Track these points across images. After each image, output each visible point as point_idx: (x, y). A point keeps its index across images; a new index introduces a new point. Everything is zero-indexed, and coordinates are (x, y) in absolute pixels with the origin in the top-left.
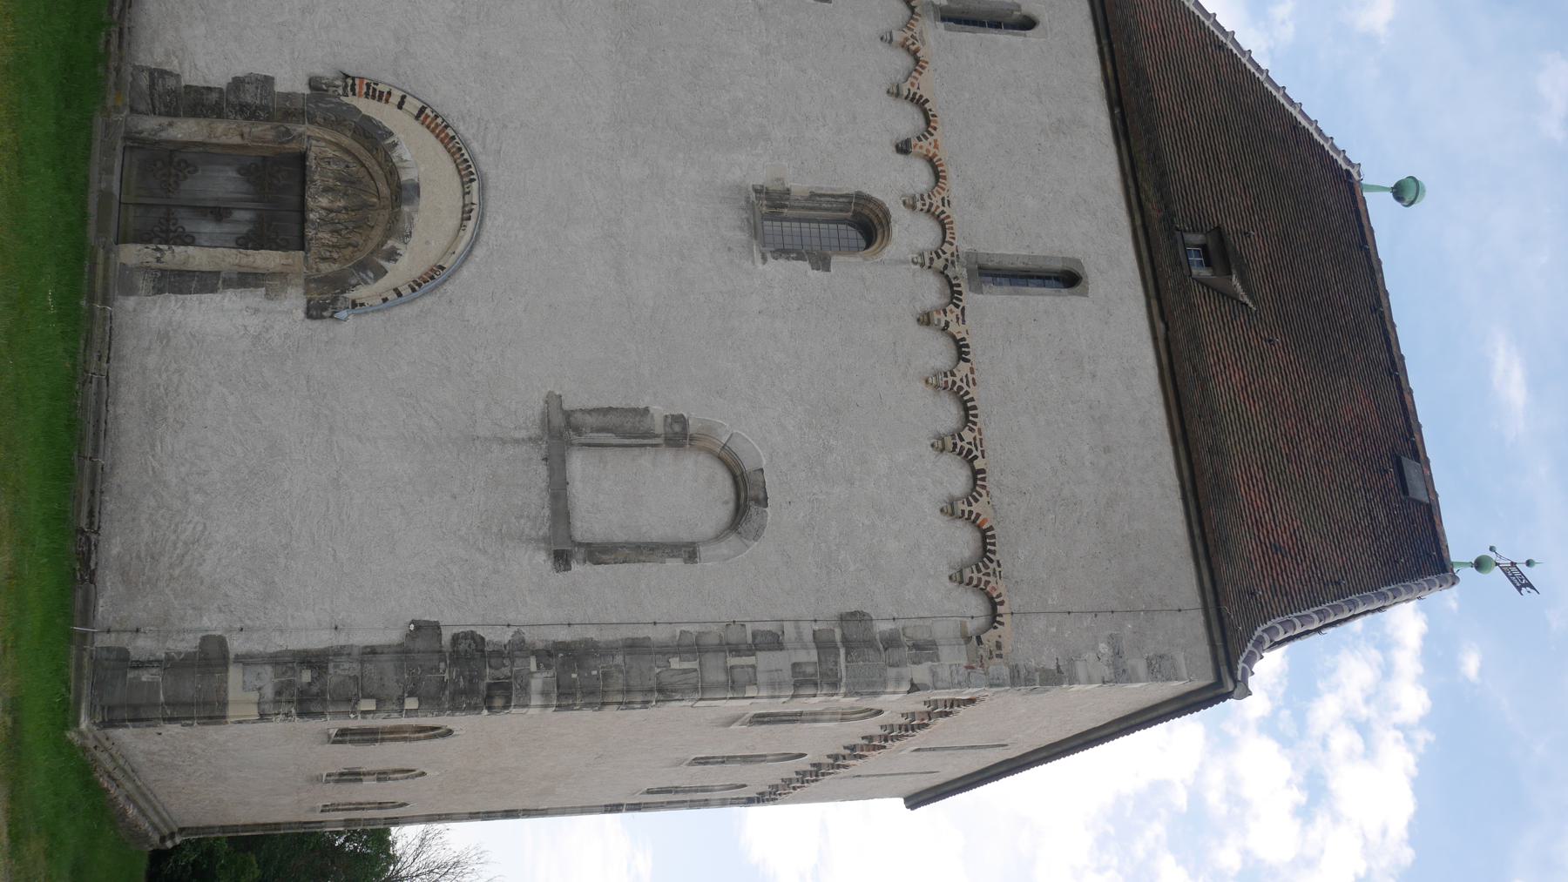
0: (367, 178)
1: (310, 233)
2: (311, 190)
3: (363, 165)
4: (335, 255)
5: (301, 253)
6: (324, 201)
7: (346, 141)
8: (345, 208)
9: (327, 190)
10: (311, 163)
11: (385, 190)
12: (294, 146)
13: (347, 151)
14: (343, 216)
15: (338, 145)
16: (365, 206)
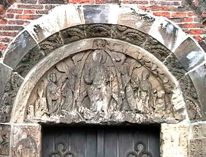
0: (69, 63)
1: (139, 118)
2: (91, 118)
3: (55, 67)
4: (161, 93)
5: (164, 126)
6: (101, 105)
7: (27, 82)
8: (108, 83)
9: (87, 100)
10: (56, 119)
11: (84, 44)
12: (38, 136)
13: (41, 80)
14: (115, 86)
15: (35, 92)
16: (102, 63)
